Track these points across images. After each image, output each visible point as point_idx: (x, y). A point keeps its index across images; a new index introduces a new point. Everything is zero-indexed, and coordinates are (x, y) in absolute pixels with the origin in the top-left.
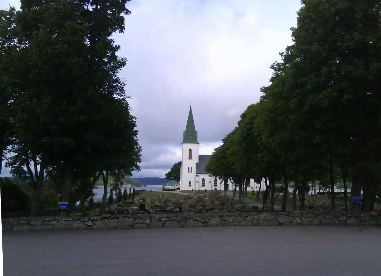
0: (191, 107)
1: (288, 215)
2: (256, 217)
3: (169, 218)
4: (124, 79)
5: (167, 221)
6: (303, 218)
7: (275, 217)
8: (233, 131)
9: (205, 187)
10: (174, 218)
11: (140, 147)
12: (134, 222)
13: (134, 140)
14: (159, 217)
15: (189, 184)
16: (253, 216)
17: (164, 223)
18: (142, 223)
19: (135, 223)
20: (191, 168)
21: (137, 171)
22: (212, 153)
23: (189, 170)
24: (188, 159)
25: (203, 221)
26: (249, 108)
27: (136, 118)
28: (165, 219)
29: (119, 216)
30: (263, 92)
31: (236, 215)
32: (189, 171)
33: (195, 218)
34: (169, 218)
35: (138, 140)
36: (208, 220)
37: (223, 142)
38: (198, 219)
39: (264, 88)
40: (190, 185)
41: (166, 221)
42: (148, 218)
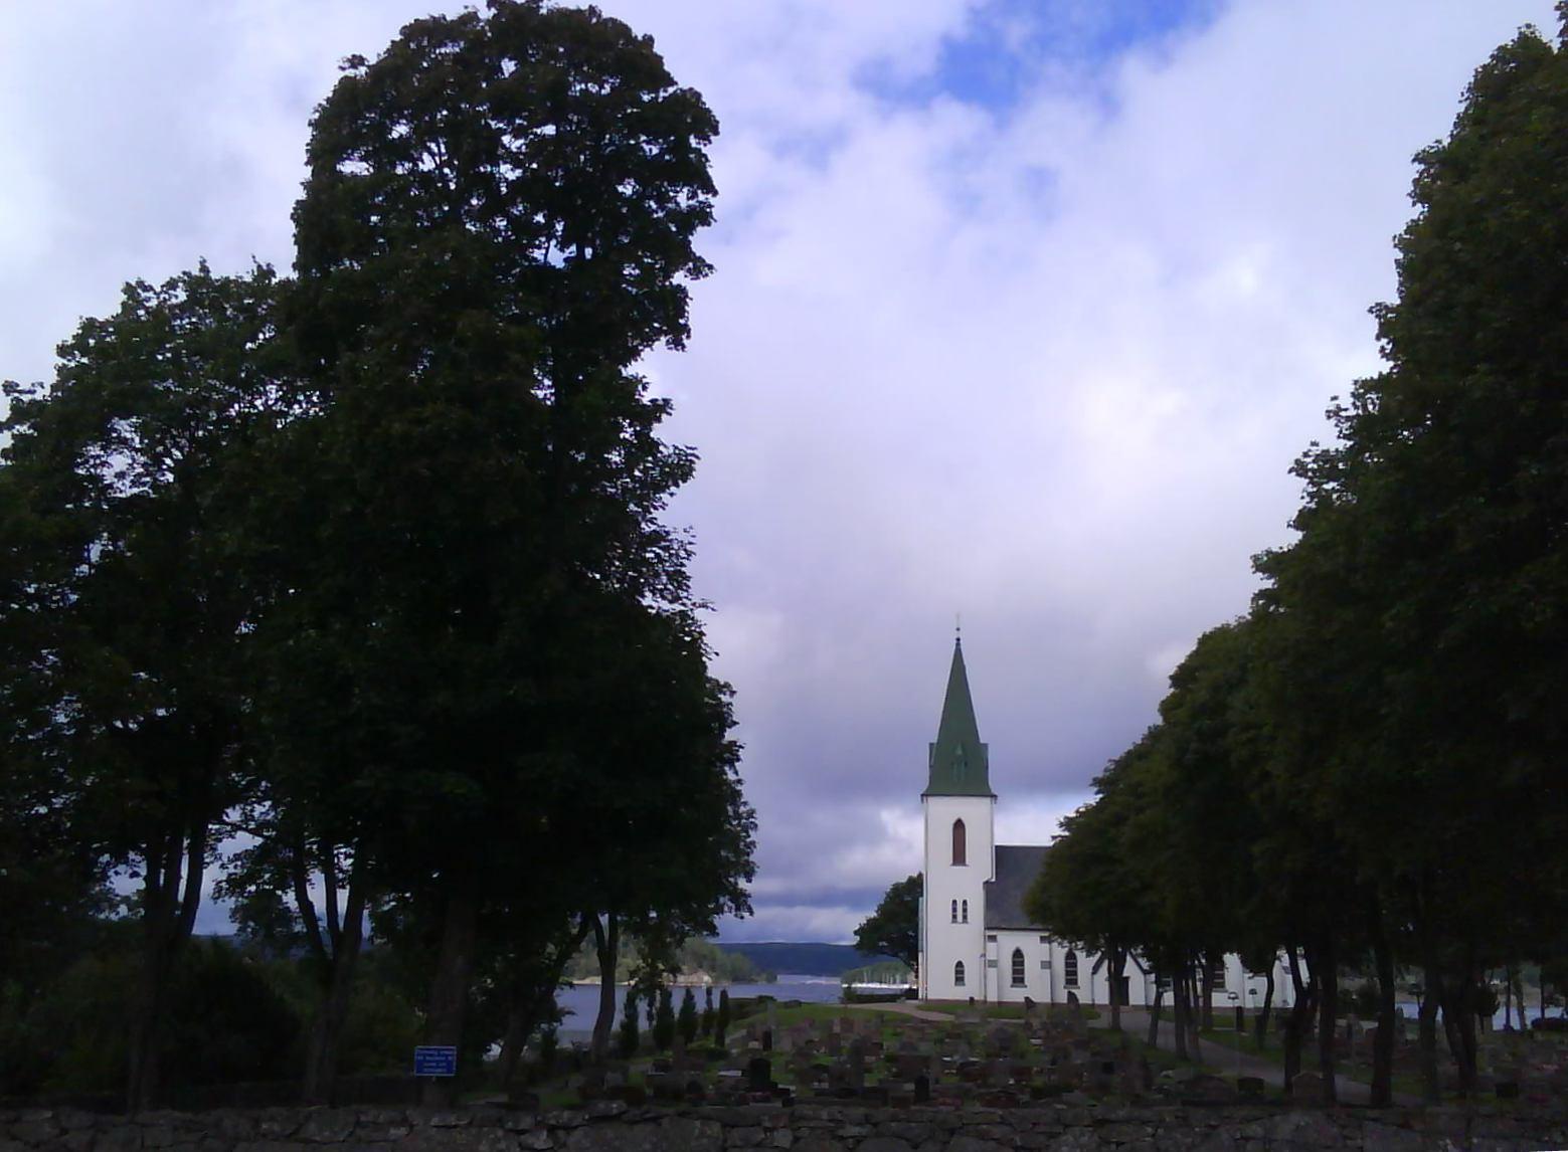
0: (958, 640)
1: (1406, 1125)
2: (1255, 1129)
3: (875, 1125)
4: (685, 531)
5: (865, 1137)
6: (1475, 1141)
7: (1345, 1132)
8: (1140, 742)
9: (1026, 987)
10: (893, 1124)
11: (751, 814)
12: (725, 1141)
13: (727, 783)
14: (830, 1121)
15: (957, 972)
16: (1241, 1123)
17: (851, 1146)
18: (759, 1145)
19: (729, 1143)
20: (965, 902)
21: (736, 915)
22: (1054, 838)
23: (955, 910)
24: (951, 862)
25: (1019, 1143)
26: (1205, 640)
27: (734, 689)
28: (855, 1130)
29: (665, 1110)
30: (1264, 573)
31: (1167, 1119)
32: (955, 917)
33: (985, 1126)
34: (875, 1125)
35: (742, 784)
36: (1042, 1138)
37: (1096, 789)
38: (998, 1131)
39: (1267, 555)
40: (962, 979)
41: (859, 1140)
42: (782, 1125)
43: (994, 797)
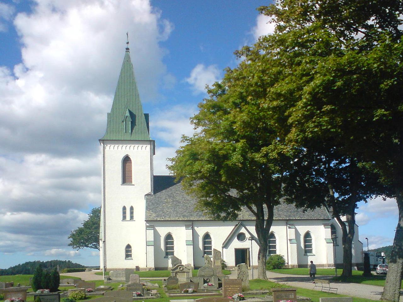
20: (132, 208)
32: (124, 218)
40: (130, 256)
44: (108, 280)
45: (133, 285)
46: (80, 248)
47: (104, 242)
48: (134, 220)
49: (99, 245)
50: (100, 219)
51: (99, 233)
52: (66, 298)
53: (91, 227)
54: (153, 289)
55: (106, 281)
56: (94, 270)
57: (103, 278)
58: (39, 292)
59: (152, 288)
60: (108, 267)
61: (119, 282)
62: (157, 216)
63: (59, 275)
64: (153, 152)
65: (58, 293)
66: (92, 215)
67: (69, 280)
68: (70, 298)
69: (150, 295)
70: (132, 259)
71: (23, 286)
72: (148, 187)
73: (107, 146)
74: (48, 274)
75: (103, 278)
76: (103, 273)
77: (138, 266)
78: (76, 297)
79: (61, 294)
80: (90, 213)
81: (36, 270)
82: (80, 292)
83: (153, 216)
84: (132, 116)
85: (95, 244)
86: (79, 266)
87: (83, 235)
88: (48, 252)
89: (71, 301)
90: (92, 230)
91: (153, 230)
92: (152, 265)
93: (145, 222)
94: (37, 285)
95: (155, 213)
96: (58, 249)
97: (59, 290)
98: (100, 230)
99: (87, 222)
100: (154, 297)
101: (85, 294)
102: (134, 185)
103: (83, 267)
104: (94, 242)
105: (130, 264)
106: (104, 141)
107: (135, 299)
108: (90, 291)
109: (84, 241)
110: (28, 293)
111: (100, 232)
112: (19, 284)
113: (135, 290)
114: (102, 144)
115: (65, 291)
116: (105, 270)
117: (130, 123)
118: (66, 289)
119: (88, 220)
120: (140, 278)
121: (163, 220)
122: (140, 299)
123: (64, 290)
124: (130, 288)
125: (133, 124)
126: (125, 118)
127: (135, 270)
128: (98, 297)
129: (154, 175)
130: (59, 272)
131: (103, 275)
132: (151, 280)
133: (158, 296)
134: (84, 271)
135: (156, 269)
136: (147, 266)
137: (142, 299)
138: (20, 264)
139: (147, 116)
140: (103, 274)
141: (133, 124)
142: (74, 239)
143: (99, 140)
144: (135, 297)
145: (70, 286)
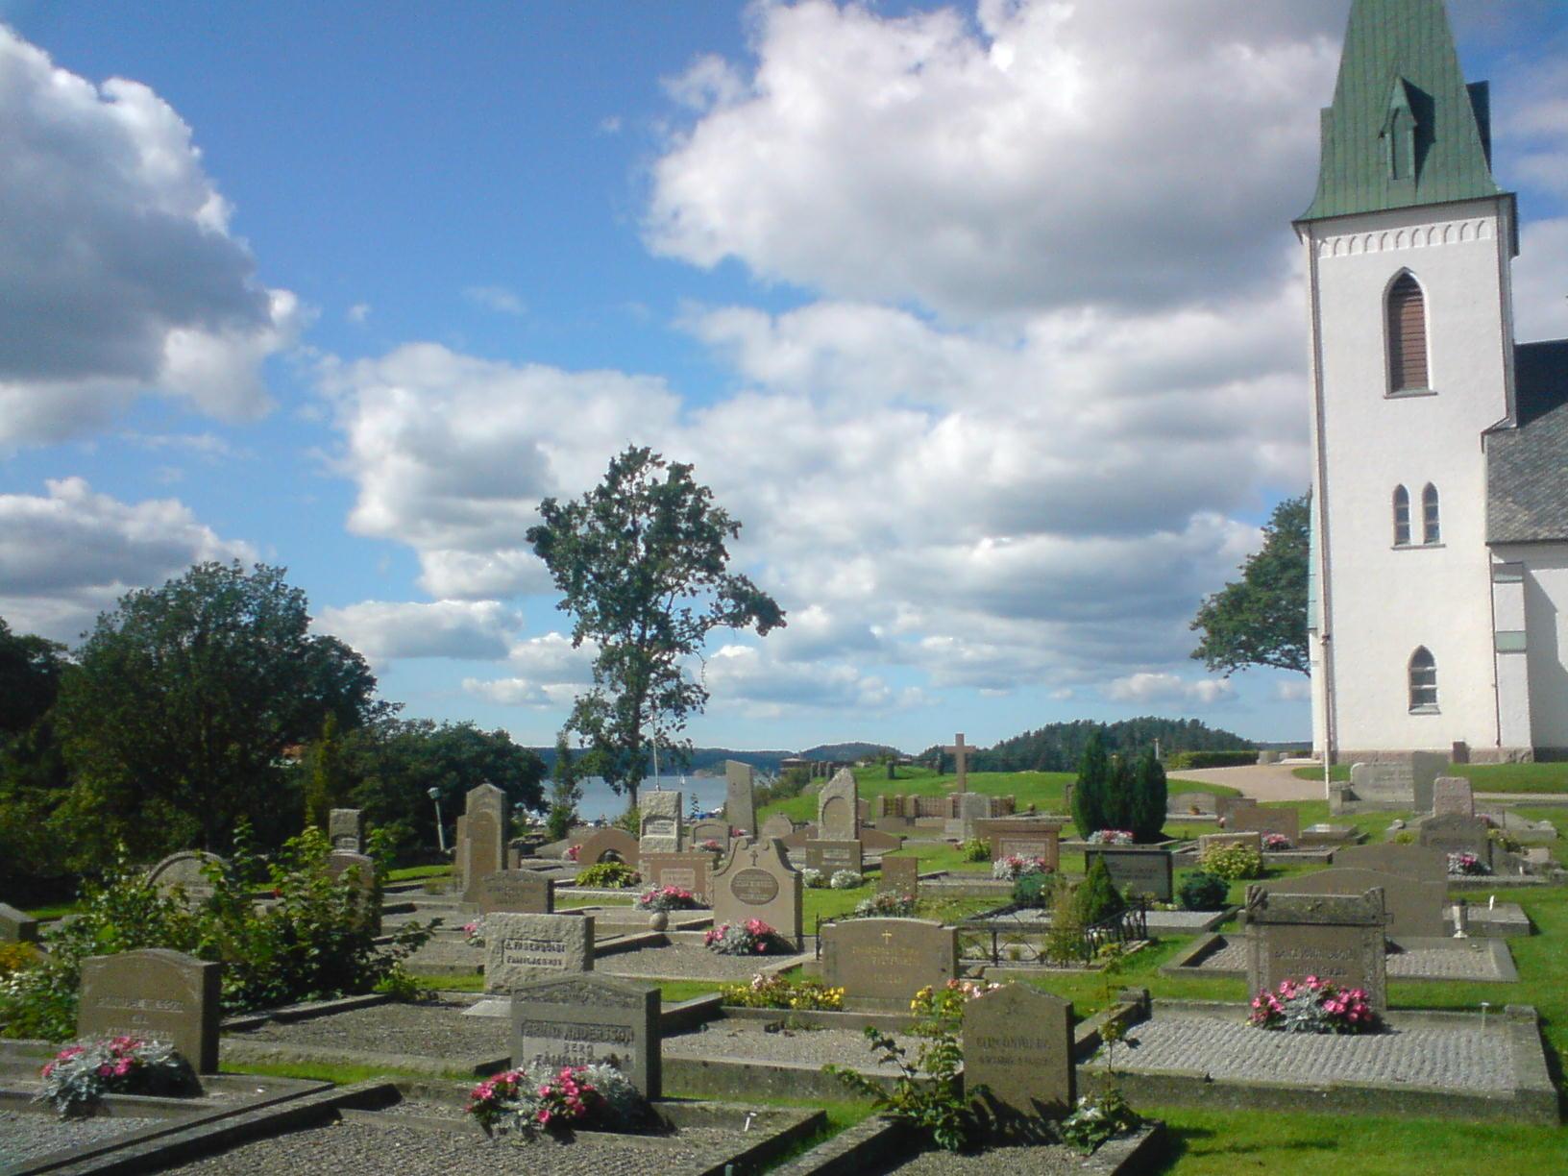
23: (1401, 515)
24: (1384, 392)
32: (1402, 534)
43: (1507, 207)
44: (1344, 800)
45: (1450, 820)
46: (1236, 668)
47: (1327, 637)
48: (1442, 541)
49: (1307, 655)
50: (1307, 544)
51: (1305, 603)
52: (1192, 871)
53: (1277, 580)
54: (1534, 845)
55: (1336, 803)
56: (1290, 757)
57: (1324, 790)
58: (1096, 838)
59: (1528, 839)
60: (1344, 745)
61: (1390, 810)
62: (1538, 522)
63: (1164, 777)
64: (1510, 245)
65: (1162, 847)
66: (1276, 530)
67: (1201, 798)
68: (1206, 871)
69: (1521, 869)
70: (1439, 713)
71: (1045, 816)
72: (1494, 403)
73: (1324, 241)
74: (1124, 771)
75: (1324, 790)
76: (1327, 770)
77: (1463, 744)
78: (1229, 868)
79: (1174, 852)
80: (1270, 523)
81: (1084, 755)
82: (1240, 846)
83: (1521, 524)
84: (1420, 103)
85: (1290, 650)
86: (1232, 740)
87: (1246, 615)
88: (1120, 688)
89: (1210, 880)
90: (1278, 592)
91: (1521, 585)
92: (1520, 738)
93: (1488, 548)
94: (1092, 818)
95: (1529, 506)
96: (1155, 672)
97: (1165, 838)
98: (1307, 592)
99: (1260, 559)
100: (1538, 879)
101: (1261, 858)
102: (1436, 394)
103: (1248, 745)
104: (1287, 643)
105: (1431, 734)
106: (1310, 225)
107: (1456, 885)
108: (1278, 846)
109: (1249, 639)
110: (1063, 840)
111: (1310, 599)
112: (1030, 805)
113: (1457, 844)
114: (1306, 238)
115: (1186, 839)
116: (1333, 756)
117: (1410, 134)
118: (1190, 836)
119: (1262, 553)
120: (1476, 795)
121: (1562, 536)
122: (1479, 884)
123: (1182, 836)
124: (1439, 836)
125: (1424, 138)
126: (1390, 120)
127: (1451, 760)
128: (1308, 871)
129: (1519, 342)
130: (1164, 766)
131: (1324, 780)
132: (1520, 806)
133: (1557, 875)
134: (1249, 760)
135: (1542, 754)
136: (1498, 742)
137: (1487, 885)
138: (1028, 733)
139: (1479, 94)
140: (1327, 776)
141: (1424, 138)
142: (1212, 632)
143: (1296, 223)
144: (1458, 878)
145: (1205, 820)
